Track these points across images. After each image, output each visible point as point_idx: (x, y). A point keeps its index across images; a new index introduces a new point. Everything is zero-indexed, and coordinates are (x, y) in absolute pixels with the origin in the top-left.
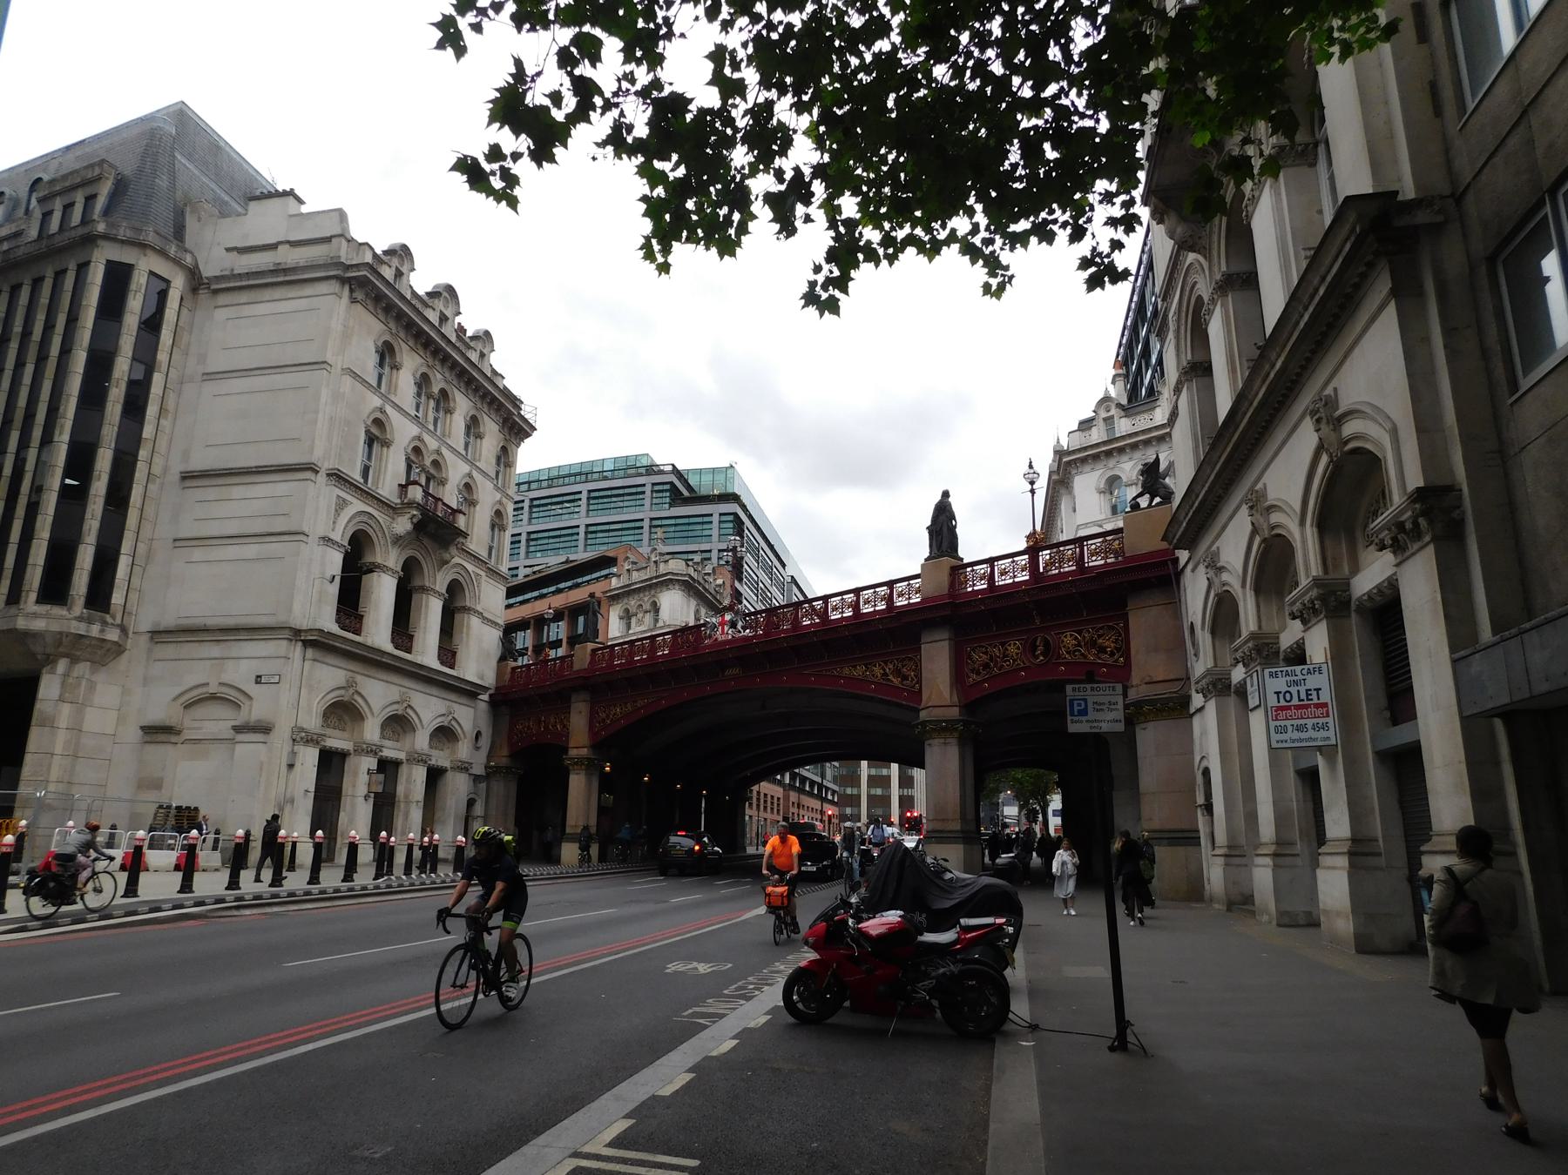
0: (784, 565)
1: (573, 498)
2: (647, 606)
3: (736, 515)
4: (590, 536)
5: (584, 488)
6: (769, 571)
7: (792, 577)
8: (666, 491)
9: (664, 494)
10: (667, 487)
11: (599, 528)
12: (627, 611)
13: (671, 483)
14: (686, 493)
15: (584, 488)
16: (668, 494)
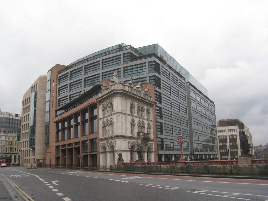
0: (184, 79)
1: (97, 64)
2: (109, 105)
3: (155, 61)
4: (104, 77)
5: (100, 59)
6: (176, 82)
7: (189, 83)
8: (129, 56)
9: (128, 57)
10: (129, 54)
11: (107, 73)
12: (104, 107)
13: (130, 53)
14: (138, 56)
15: (100, 59)
16: (129, 57)
